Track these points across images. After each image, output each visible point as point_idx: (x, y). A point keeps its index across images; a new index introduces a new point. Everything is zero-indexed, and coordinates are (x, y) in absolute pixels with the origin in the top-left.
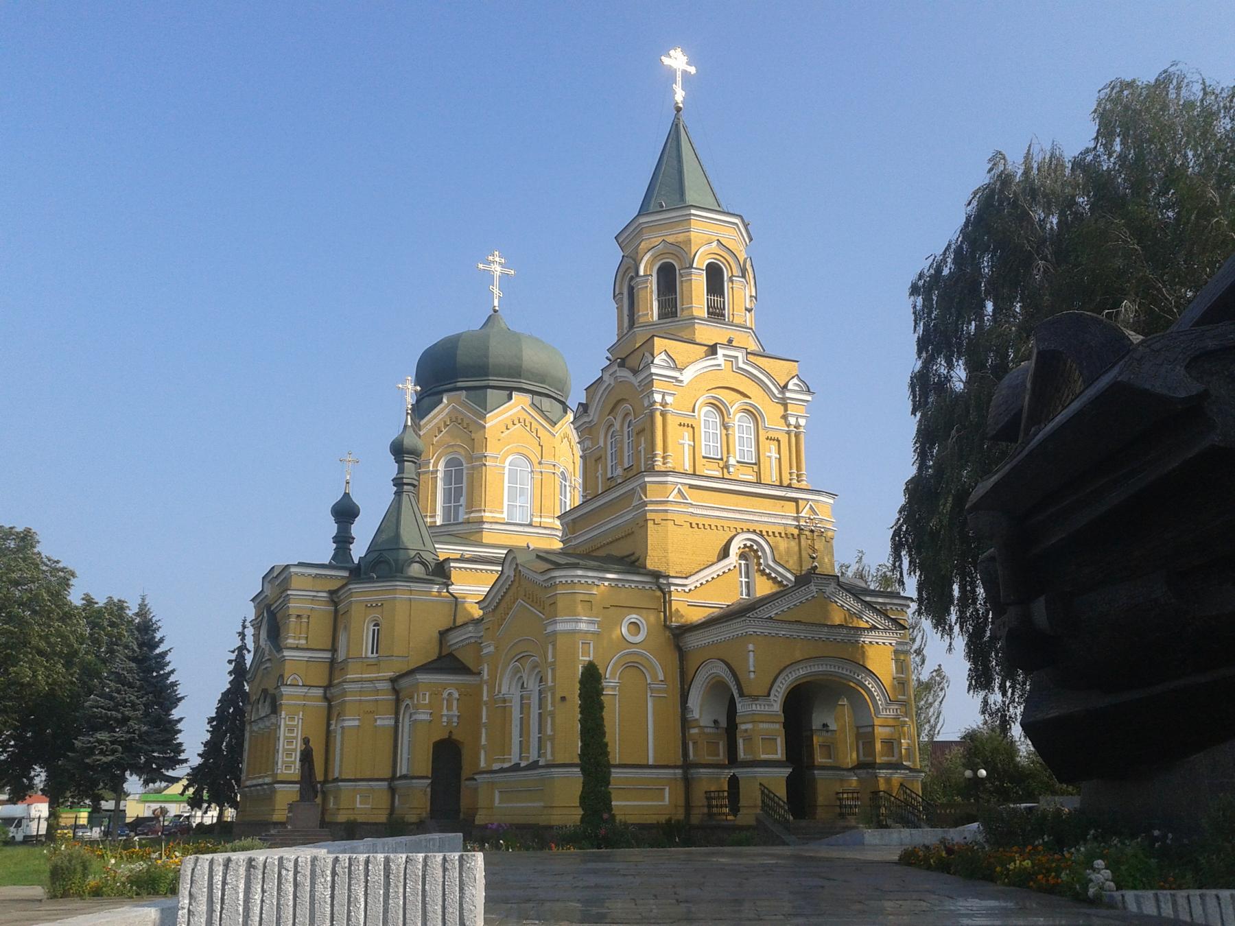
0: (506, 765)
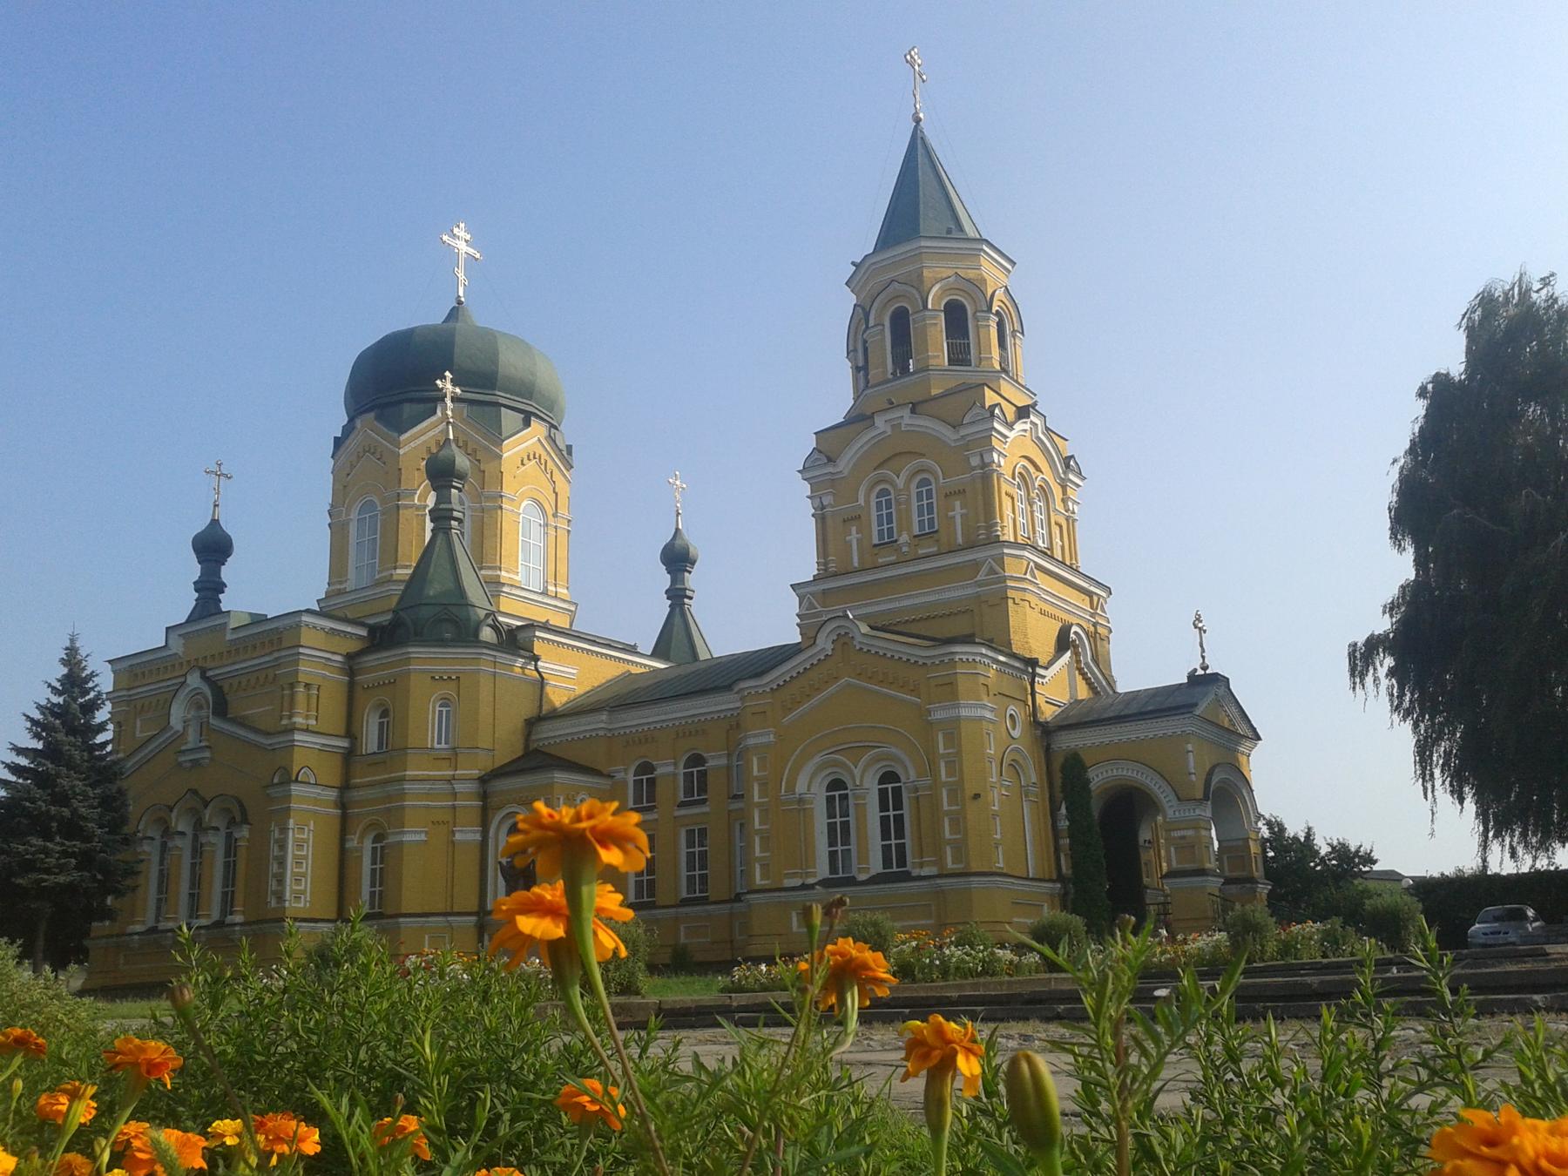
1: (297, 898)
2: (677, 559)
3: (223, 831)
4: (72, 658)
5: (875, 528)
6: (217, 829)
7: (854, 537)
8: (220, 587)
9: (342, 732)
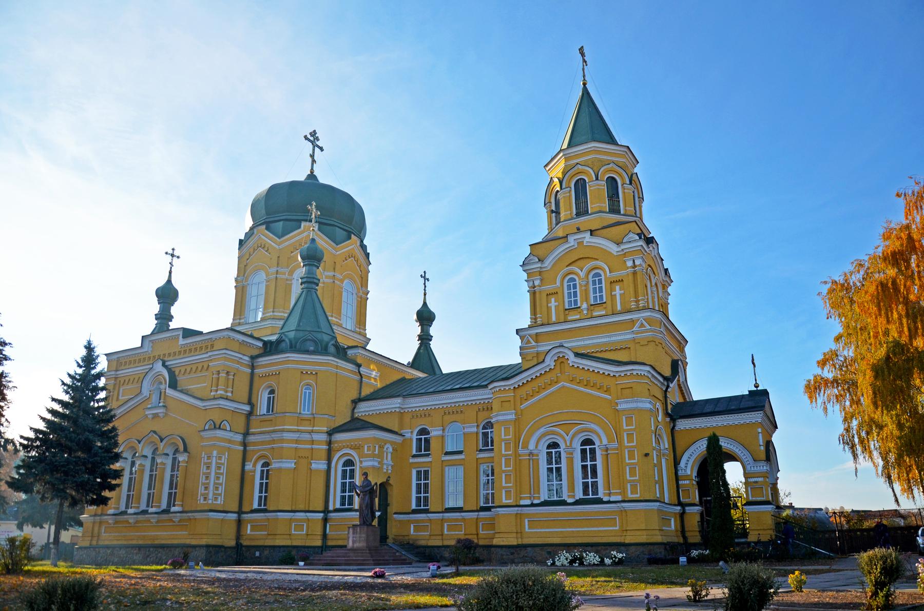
0: (536, 502)
1: (216, 499)
2: (425, 317)
3: (171, 457)
4: (89, 348)
5: (566, 300)
6: (167, 455)
7: (553, 304)
8: (171, 318)
9: (246, 401)
